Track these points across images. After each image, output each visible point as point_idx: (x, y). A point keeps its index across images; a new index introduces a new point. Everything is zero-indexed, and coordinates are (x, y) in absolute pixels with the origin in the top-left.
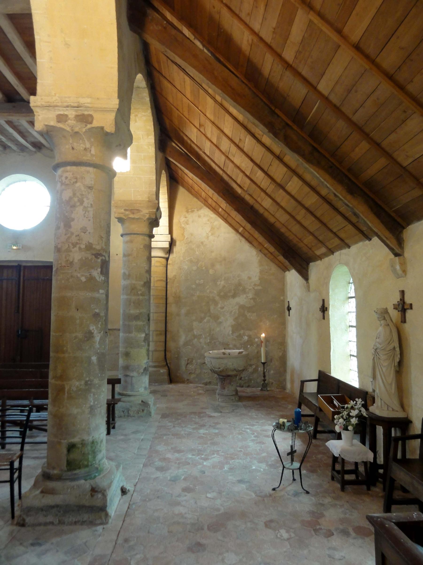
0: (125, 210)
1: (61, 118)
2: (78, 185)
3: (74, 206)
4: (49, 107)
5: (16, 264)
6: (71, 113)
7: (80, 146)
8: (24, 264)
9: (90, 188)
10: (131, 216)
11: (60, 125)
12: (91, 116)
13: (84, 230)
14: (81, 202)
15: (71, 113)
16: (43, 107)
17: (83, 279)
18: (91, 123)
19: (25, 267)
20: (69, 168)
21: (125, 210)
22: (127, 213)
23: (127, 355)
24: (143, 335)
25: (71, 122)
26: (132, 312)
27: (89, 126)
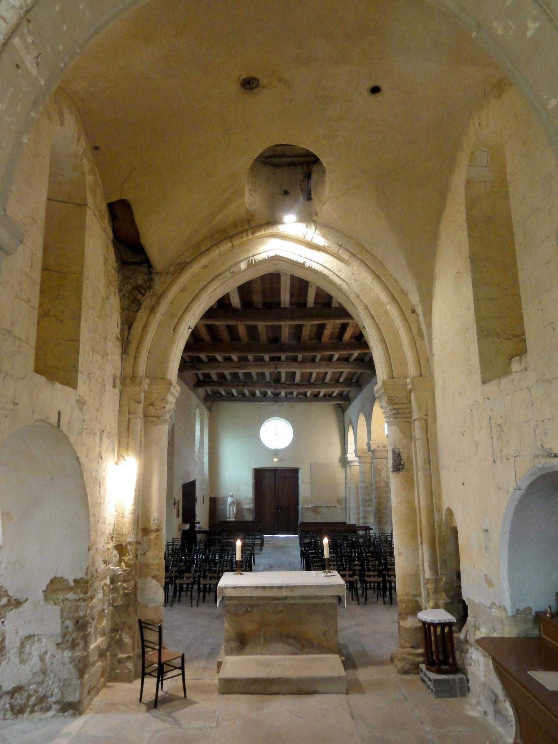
0: (363, 452)
1: (378, 447)
2: (382, 464)
3: (381, 470)
4: (375, 444)
5: (273, 469)
6: (381, 445)
7: (382, 453)
8: (277, 469)
9: (385, 465)
10: (365, 455)
11: (378, 449)
12: (386, 446)
13: (384, 476)
14: (383, 469)
15: (381, 445)
16: (373, 444)
17: (385, 491)
18: (386, 448)
19: (278, 470)
20: (379, 459)
21: (363, 452)
22: (363, 454)
23: (365, 517)
24: (371, 509)
25: (381, 448)
26: (367, 498)
27: (385, 449)
